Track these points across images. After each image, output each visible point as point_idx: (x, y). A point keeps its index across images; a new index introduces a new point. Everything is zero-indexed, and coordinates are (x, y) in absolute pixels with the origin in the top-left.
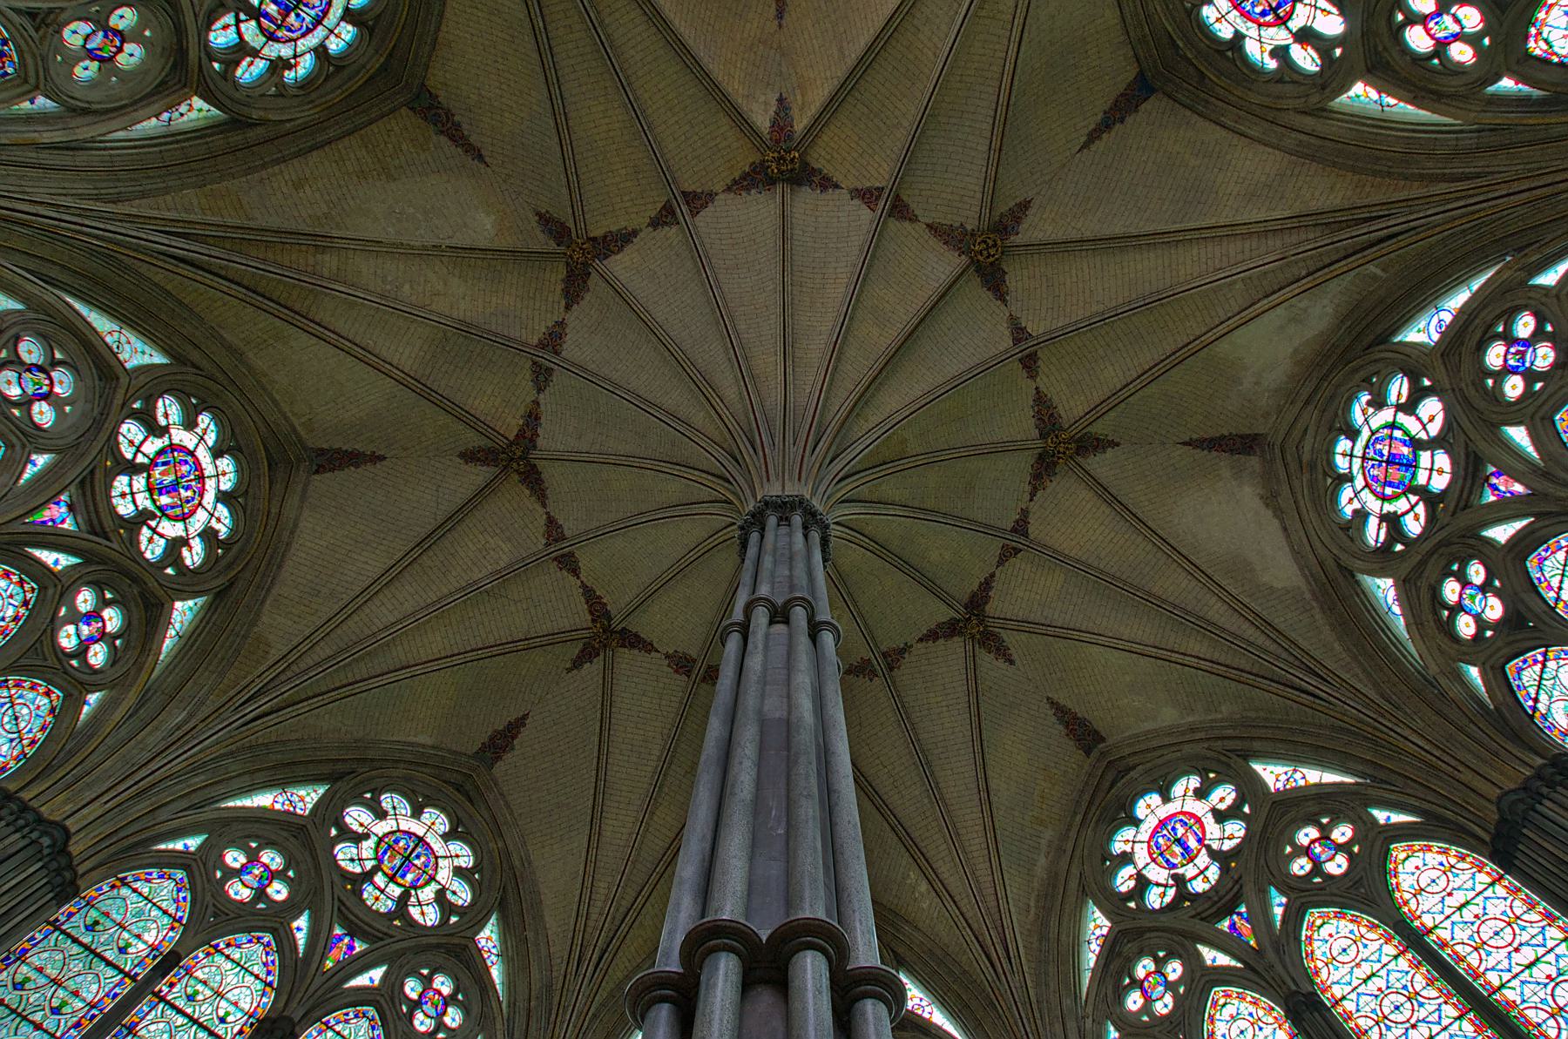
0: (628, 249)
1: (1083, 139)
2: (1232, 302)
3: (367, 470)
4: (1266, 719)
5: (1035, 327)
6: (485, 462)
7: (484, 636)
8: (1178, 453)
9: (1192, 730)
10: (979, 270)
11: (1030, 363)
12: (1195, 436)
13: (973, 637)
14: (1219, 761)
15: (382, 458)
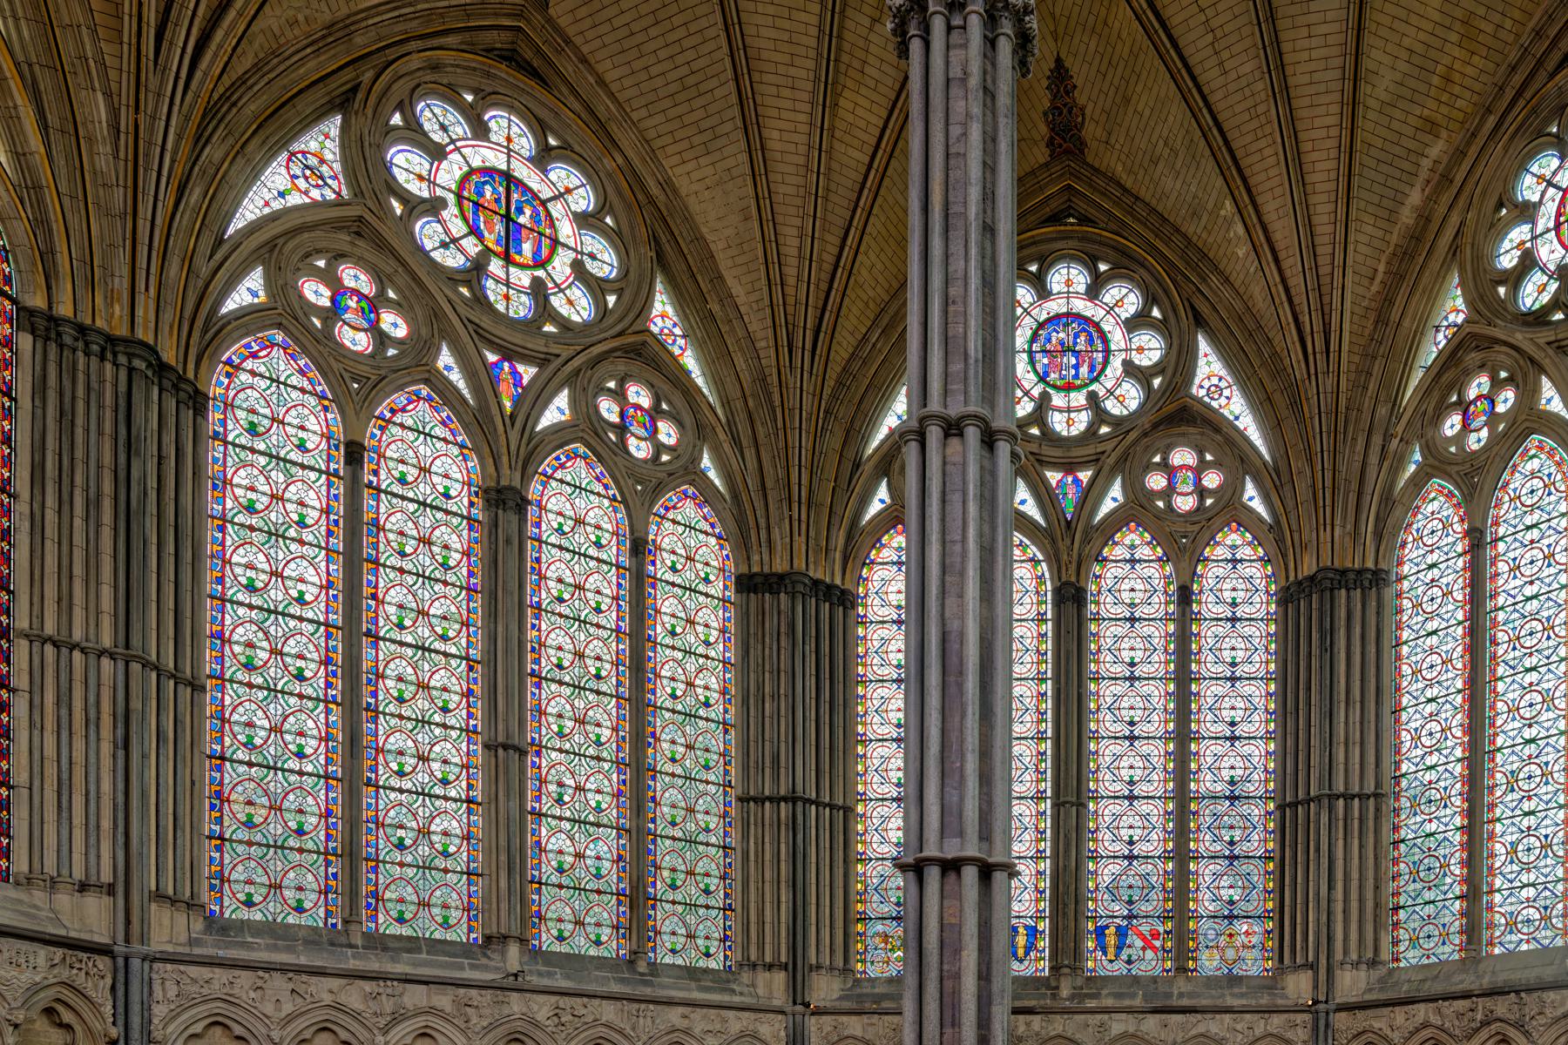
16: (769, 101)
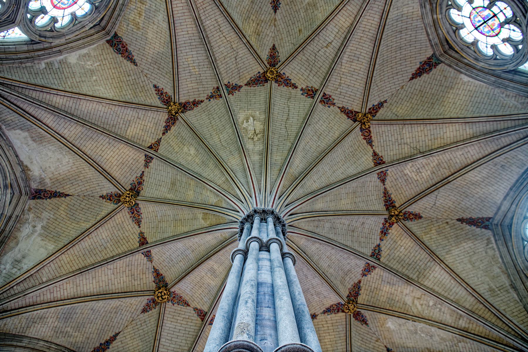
0: (328, 306)
1: (118, 337)
2: (47, 271)
3: (466, 216)
4: (21, 63)
5: (139, 257)
6: (411, 213)
7: (426, 129)
8: (71, 191)
9: (60, 51)
10: (166, 285)
11: (143, 241)
12: (63, 199)
13: (175, 103)
14: (45, 37)
15: (458, 220)
16: (374, 29)
